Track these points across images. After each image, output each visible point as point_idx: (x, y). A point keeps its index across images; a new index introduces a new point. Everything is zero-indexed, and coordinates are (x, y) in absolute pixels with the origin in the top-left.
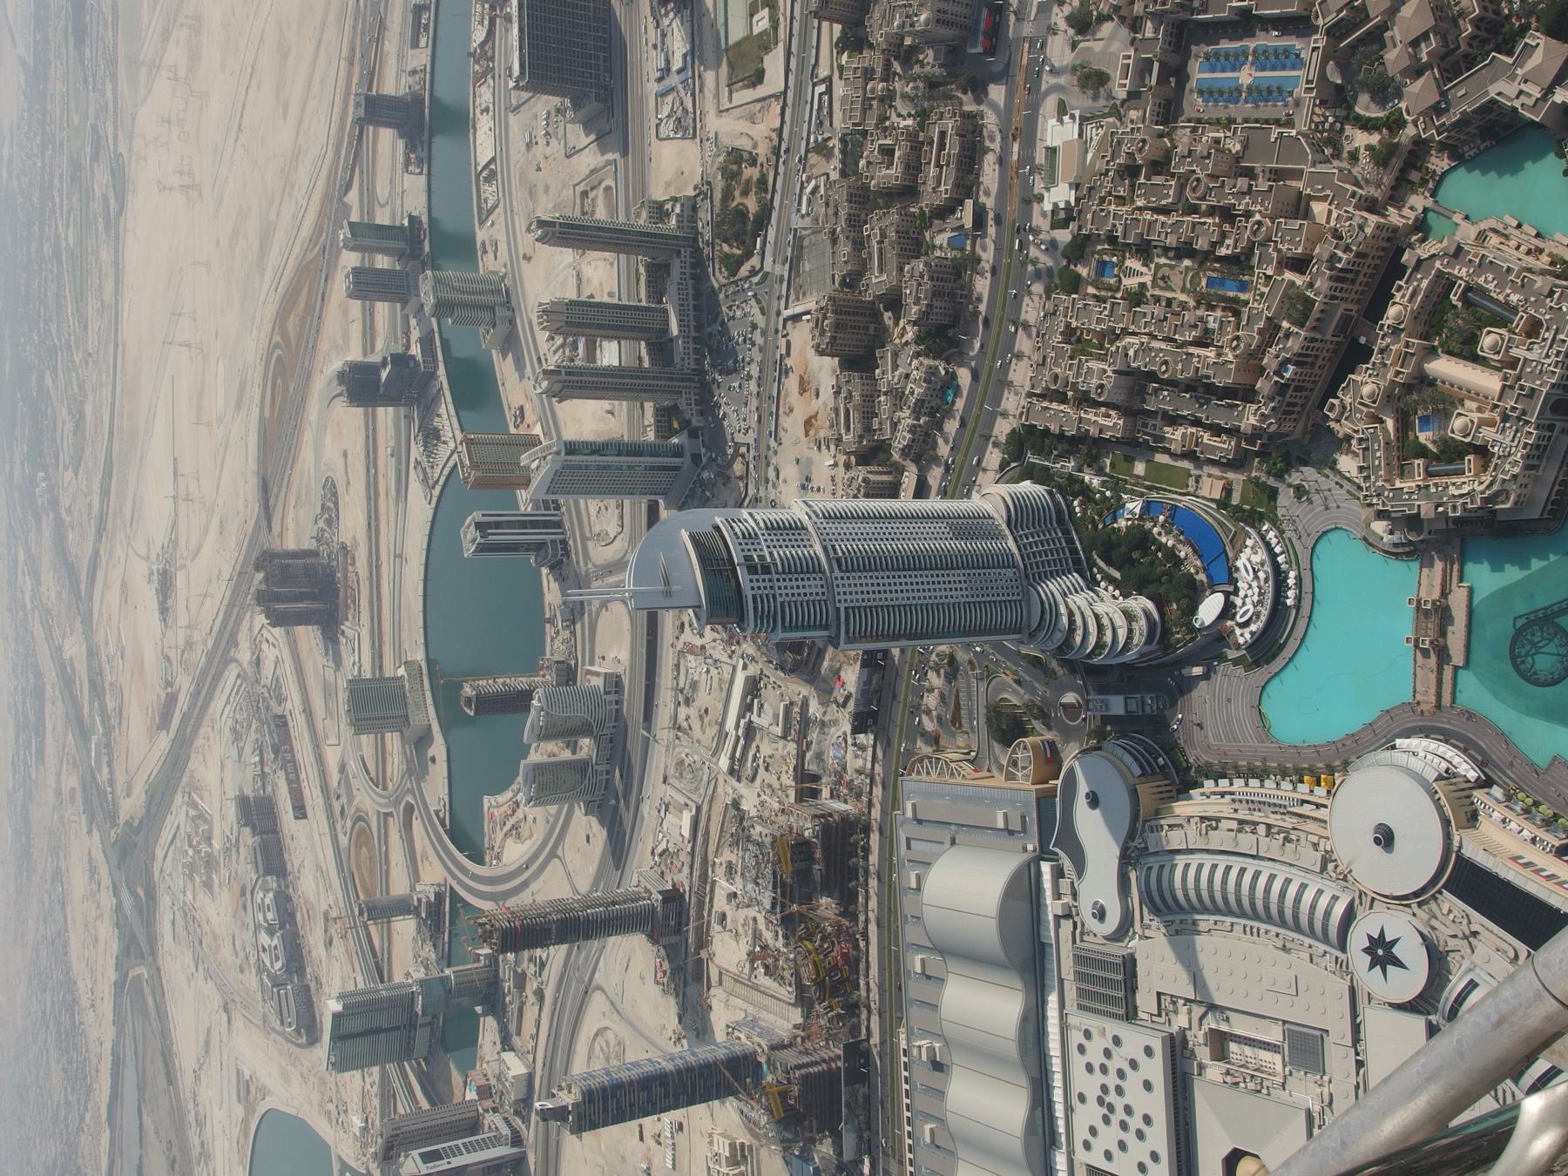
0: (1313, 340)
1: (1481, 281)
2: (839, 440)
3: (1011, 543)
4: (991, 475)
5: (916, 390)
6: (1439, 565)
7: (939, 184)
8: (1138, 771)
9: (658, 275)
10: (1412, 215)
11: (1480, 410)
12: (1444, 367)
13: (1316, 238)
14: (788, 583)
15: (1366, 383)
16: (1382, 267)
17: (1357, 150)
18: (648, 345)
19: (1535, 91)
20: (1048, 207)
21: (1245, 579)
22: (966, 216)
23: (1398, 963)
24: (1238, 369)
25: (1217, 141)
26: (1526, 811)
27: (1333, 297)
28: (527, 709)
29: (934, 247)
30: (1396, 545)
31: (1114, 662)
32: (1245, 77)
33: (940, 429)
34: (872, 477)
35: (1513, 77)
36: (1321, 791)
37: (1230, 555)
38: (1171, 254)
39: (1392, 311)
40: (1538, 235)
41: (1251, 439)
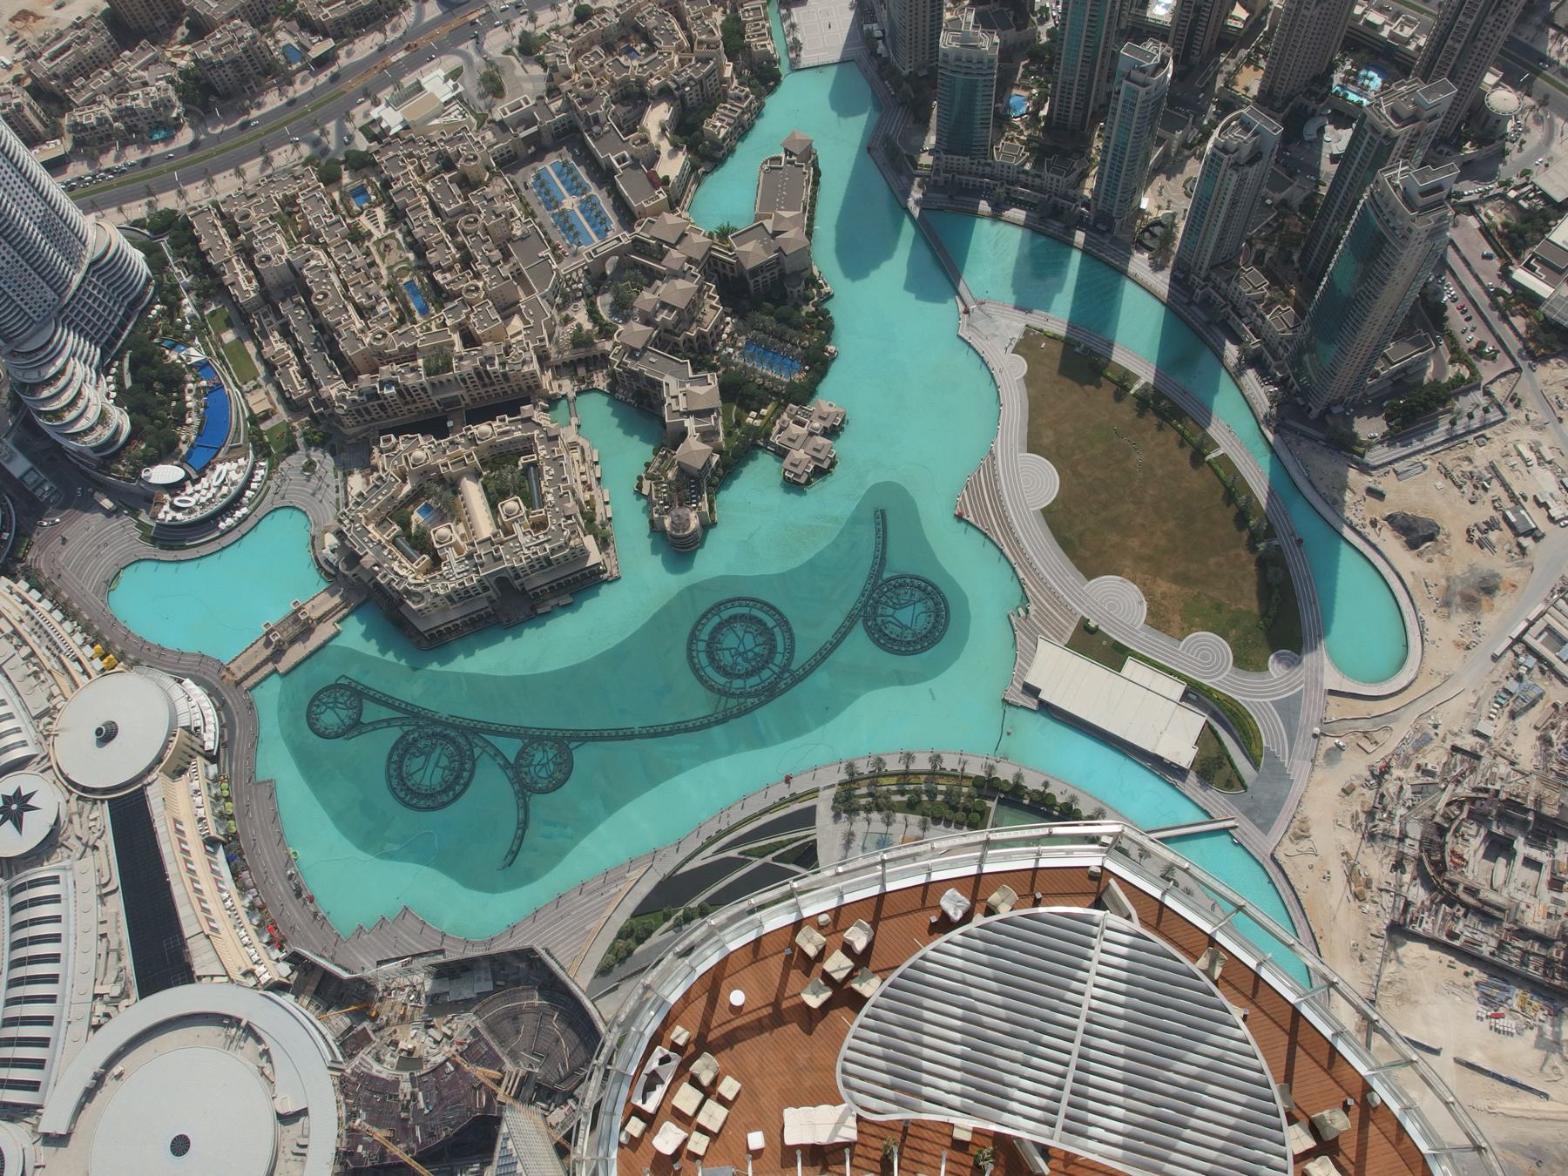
0: (424, 390)
1: (546, 468)
2: (34, 56)
3: (77, 278)
4: (121, 220)
6: (337, 600)
10: (556, 390)
11: (462, 537)
12: (473, 492)
15: (422, 450)
16: (508, 397)
17: (573, 319)
20: (375, 114)
21: (211, 480)
22: (319, 47)
23: (18, 825)
24: (362, 353)
25: (512, 214)
26: (217, 798)
27: (464, 380)
29: (273, 35)
30: (327, 561)
31: (54, 436)
32: (570, 203)
33: (124, 146)
34: (27, 111)
35: (682, 385)
36: (98, 664)
37: (220, 456)
38: (409, 239)
39: (484, 428)
40: (598, 479)
41: (320, 402)
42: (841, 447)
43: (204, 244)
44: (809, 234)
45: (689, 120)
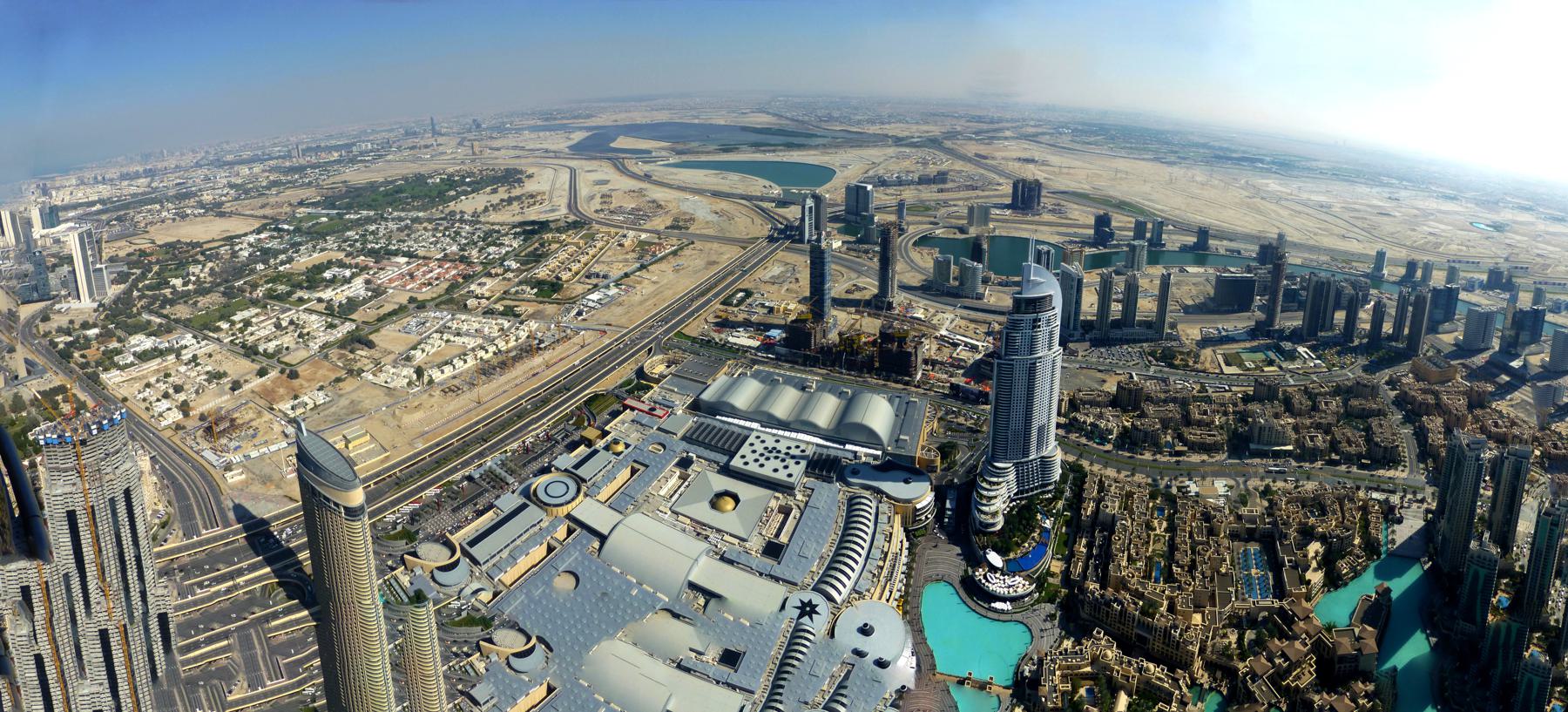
5: (1102, 424)
9: (1148, 325)
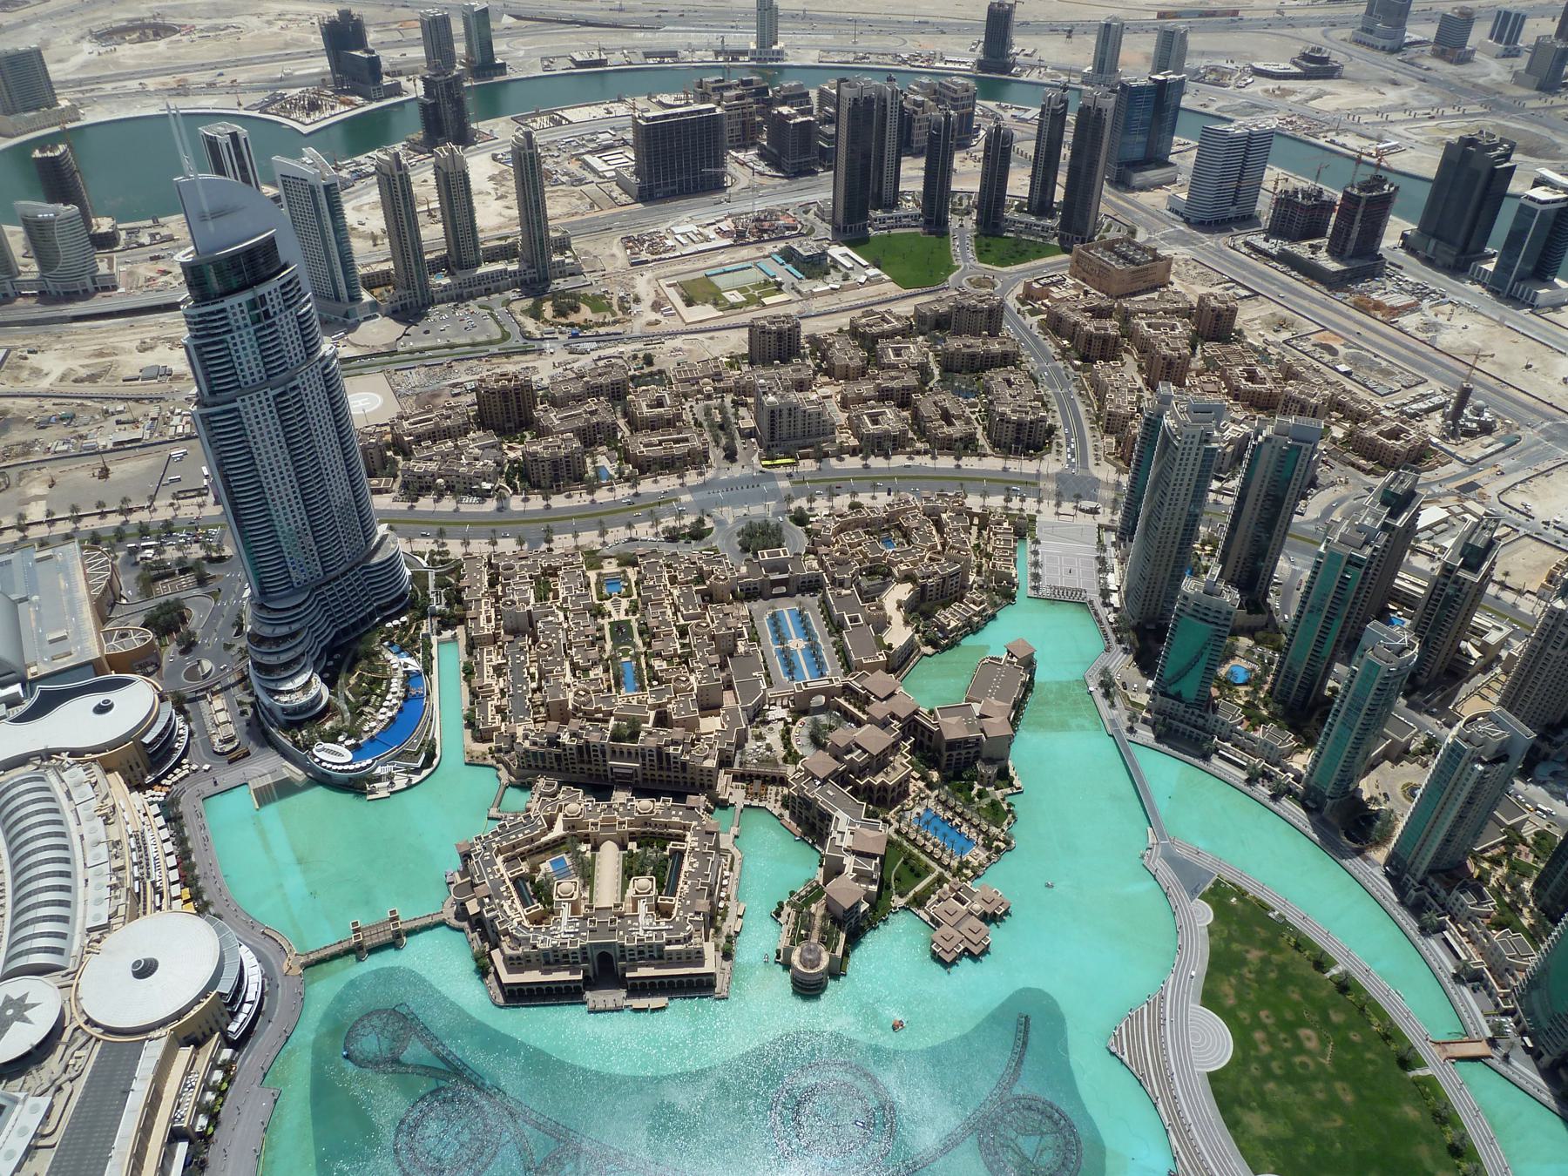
0: (604, 753)
7: (646, 446)
8: (147, 740)
13: (691, 725)
14: (249, 351)
15: (577, 804)
18: (445, 257)
19: (847, 842)
25: (741, 635)
27: (644, 757)
28: (52, 199)
29: (593, 456)
32: (797, 644)
33: (440, 496)
39: (645, 803)
42: (995, 935)
43: (463, 583)
44: (1014, 723)
45: (924, 607)
